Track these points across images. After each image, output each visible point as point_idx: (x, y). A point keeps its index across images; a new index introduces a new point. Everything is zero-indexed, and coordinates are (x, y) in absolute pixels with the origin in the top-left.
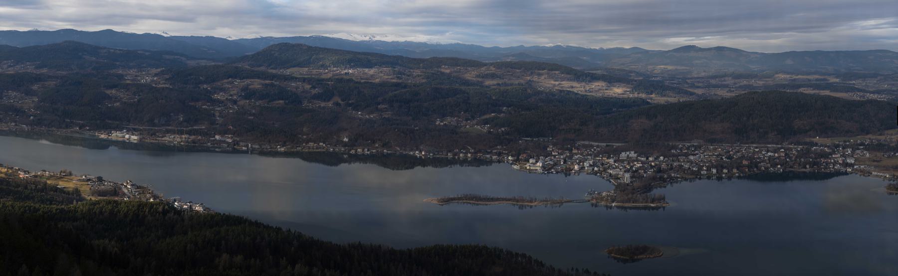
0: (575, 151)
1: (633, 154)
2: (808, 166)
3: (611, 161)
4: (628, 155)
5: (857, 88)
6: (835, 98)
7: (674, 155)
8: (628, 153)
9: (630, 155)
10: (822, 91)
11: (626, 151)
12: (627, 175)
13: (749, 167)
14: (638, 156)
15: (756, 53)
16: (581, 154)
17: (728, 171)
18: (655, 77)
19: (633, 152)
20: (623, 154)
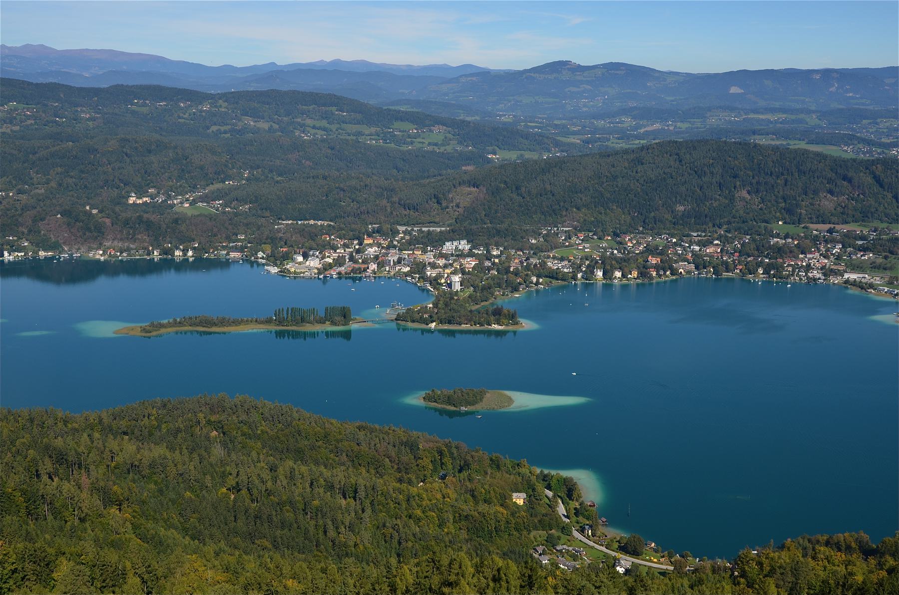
0: (368, 241)
1: (464, 245)
2: (761, 271)
3: (429, 257)
4: (457, 248)
5: (858, 138)
6: (818, 154)
7: (532, 247)
8: (455, 243)
9: (460, 247)
10: (791, 142)
11: (452, 240)
12: (456, 279)
13: (657, 267)
14: (474, 247)
15: (677, 74)
16: (379, 245)
17: (622, 275)
18: (501, 116)
19: (463, 242)
20: (448, 244)
